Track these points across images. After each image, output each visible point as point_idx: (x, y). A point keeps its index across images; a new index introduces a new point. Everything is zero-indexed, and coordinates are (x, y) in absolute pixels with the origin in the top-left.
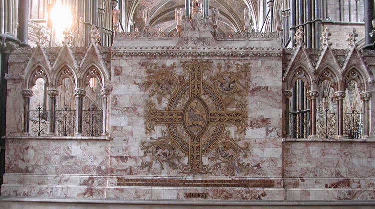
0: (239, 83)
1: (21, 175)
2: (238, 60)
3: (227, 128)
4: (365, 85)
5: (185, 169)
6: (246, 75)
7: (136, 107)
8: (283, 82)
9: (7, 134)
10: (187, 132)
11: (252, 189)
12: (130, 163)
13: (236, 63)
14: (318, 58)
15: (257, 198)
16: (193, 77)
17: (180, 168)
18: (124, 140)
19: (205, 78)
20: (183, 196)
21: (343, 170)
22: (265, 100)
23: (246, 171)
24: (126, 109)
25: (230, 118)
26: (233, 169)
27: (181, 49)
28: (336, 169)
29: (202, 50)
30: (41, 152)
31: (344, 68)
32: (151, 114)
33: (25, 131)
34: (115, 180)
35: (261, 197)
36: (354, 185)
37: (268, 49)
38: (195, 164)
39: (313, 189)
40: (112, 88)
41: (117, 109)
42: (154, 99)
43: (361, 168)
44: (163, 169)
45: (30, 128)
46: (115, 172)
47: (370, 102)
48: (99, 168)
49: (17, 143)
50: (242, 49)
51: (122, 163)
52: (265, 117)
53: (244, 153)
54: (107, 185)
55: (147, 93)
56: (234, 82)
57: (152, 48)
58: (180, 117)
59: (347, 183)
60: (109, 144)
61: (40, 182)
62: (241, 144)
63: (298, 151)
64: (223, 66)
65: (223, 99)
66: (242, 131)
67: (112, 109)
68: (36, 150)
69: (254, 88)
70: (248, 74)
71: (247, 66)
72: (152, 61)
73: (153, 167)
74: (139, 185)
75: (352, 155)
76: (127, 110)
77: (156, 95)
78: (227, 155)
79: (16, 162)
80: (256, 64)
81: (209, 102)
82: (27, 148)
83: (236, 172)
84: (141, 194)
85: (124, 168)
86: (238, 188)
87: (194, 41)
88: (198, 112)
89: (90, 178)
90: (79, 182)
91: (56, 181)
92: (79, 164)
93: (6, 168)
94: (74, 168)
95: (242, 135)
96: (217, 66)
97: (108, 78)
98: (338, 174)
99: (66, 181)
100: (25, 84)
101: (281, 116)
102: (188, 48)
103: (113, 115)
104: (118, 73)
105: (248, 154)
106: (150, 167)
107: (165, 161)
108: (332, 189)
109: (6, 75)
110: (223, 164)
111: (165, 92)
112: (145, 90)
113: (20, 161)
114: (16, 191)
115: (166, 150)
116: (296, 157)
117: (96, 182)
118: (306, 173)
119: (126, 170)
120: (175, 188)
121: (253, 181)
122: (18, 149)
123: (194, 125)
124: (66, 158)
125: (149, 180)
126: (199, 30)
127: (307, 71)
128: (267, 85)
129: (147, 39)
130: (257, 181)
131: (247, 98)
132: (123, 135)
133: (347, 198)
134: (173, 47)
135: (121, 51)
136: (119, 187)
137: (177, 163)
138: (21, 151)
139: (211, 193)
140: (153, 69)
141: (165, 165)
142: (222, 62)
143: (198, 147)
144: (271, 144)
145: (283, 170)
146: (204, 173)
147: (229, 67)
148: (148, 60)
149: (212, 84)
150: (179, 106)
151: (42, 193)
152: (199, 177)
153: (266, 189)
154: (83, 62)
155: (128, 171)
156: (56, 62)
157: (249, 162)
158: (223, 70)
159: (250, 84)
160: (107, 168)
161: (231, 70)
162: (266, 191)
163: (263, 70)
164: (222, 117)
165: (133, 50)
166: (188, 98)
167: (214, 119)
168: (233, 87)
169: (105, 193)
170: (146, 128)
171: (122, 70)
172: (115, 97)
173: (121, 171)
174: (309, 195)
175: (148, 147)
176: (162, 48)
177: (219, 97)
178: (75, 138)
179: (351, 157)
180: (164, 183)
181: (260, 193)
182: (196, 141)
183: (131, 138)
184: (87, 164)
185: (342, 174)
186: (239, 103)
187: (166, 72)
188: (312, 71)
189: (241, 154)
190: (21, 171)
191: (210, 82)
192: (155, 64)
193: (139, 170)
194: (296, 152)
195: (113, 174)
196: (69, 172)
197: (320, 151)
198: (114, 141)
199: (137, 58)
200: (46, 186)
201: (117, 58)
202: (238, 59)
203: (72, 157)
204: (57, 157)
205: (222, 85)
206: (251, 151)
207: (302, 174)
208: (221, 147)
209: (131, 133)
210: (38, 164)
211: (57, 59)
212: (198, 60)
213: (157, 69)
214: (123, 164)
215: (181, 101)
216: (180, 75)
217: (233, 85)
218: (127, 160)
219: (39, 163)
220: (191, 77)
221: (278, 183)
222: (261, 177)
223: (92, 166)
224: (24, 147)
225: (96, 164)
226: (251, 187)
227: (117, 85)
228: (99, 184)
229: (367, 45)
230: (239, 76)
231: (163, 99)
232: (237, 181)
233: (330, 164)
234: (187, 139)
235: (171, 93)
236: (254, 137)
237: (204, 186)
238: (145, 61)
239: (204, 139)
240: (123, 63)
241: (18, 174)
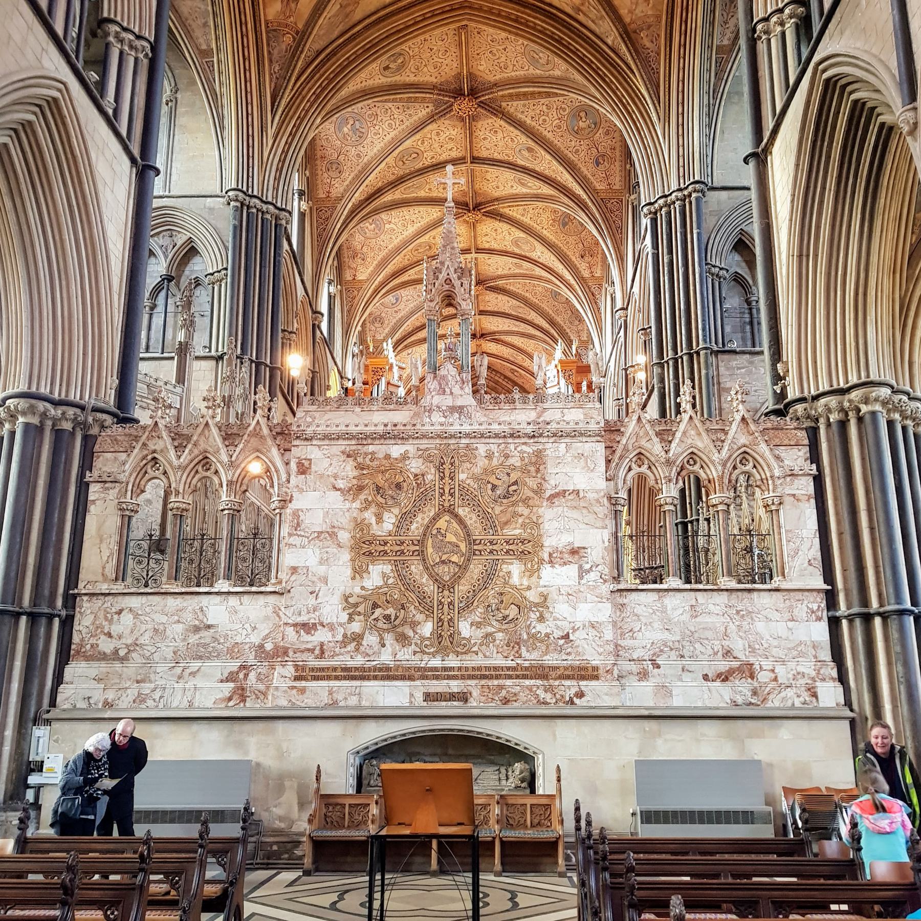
0: (525, 484)
1: (102, 667)
2: (523, 444)
3: (504, 566)
4: (770, 482)
5: (426, 646)
6: (538, 471)
7: (336, 530)
8: (607, 480)
9: (81, 585)
10: (431, 576)
11: (557, 683)
12: (321, 636)
13: (519, 449)
14: (674, 434)
15: (567, 703)
16: (442, 475)
17: (416, 644)
18: (311, 593)
19: (462, 476)
20: (422, 699)
21: (739, 646)
22: (575, 514)
23: (544, 648)
24: (316, 535)
25: (511, 547)
26: (518, 644)
27: (418, 427)
28: (724, 642)
29: (456, 428)
30: (147, 619)
31: (725, 453)
32: (364, 543)
33: (117, 579)
34: (290, 670)
35: (575, 699)
36: (764, 677)
37: (577, 423)
38: (445, 634)
39: (679, 684)
40: (292, 496)
41: (298, 536)
42: (369, 516)
43: (775, 643)
44: (383, 645)
45: (129, 572)
46: (291, 653)
47: (781, 512)
48: (261, 646)
49: (100, 603)
50: (529, 424)
51: (305, 637)
52: (576, 545)
53: (538, 614)
54: (275, 681)
55: (357, 504)
56: (513, 484)
57: (366, 426)
58: (417, 548)
59: (748, 671)
60: (281, 601)
61: (139, 678)
62: (532, 596)
63: (644, 609)
64: (496, 454)
65: (497, 513)
66: (533, 572)
67: (290, 535)
68: (136, 616)
69: (553, 492)
70: (541, 468)
71: (539, 454)
72: (366, 447)
73: (364, 643)
74: (337, 678)
75: (754, 615)
76: (318, 537)
77: (373, 509)
78: (505, 618)
80: (554, 450)
81: (471, 519)
82: (120, 612)
83: (523, 649)
84: (340, 697)
85: (310, 646)
86: (527, 682)
87: (443, 412)
88: (451, 538)
89: (243, 667)
90: (219, 677)
91: (173, 675)
92: (222, 641)
93: (72, 652)
95: (534, 579)
96: (484, 454)
97: (284, 480)
98: (728, 653)
99: (193, 674)
100: (124, 490)
101: (607, 544)
102: (432, 425)
103: (290, 545)
104: (303, 469)
105: (547, 615)
106: (359, 644)
107: (388, 631)
108: (718, 683)
109: (88, 474)
110: (500, 636)
111: (390, 502)
112: (354, 500)
113: (103, 637)
114: (89, 698)
115: (391, 610)
116: (639, 620)
117: (252, 676)
118: (661, 651)
119: (312, 651)
120: (408, 683)
121: (558, 668)
122: (101, 615)
123: (443, 562)
124: (197, 629)
125: (357, 669)
126: (452, 393)
127: (653, 459)
128: (577, 487)
129: (358, 409)
130: (566, 669)
131: (541, 511)
132: (310, 584)
133: (751, 704)
134: (405, 422)
135: (309, 431)
136: (297, 684)
137: (411, 634)
138: (106, 619)
139: (476, 693)
140: (369, 463)
141: (389, 638)
142: (494, 448)
143: (450, 603)
144: (589, 596)
145: (616, 645)
146: (462, 653)
147: (507, 457)
148: (360, 447)
149: (476, 486)
150: (416, 527)
151: (143, 701)
152: (453, 661)
153: (582, 683)
154: (238, 450)
155: (317, 652)
156: (187, 451)
157: (548, 631)
158: (495, 462)
159: (546, 486)
160: (276, 647)
161: (511, 461)
162: (583, 688)
163: (570, 459)
164: (495, 547)
165: (333, 429)
166: (432, 514)
167: (480, 551)
168: (515, 491)
169: (270, 697)
170: (355, 571)
171: (310, 464)
172: (296, 514)
173: (302, 652)
174: (671, 695)
175: (356, 605)
176: (386, 425)
177: (490, 511)
178: (216, 590)
179: (752, 619)
180: (386, 674)
181: (573, 691)
182: (446, 593)
183: (324, 588)
184: (239, 639)
185: (735, 654)
186: (527, 521)
187: (392, 465)
188: (663, 460)
189: (532, 615)
190: (103, 657)
191: (472, 484)
192: (373, 453)
193: (337, 650)
194: (639, 610)
195: (287, 659)
196: (200, 658)
197: (687, 608)
198: (291, 594)
199: (341, 442)
200: (152, 685)
201: (303, 443)
202: (523, 440)
203: (209, 627)
204: (179, 628)
205: (494, 488)
206: (551, 609)
207: (654, 654)
208: (494, 601)
209: (325, 580)
210: (138, 642)
211: (190, 446)
212: (449, 445)
213: (376, 463)
214: (308, 638)
215: (419, 519)
216: (417, 471)
217: (514, 488)
218: (316, 630)
219: (141, 641)
220: (437, 476)
221: (607, 671)
222: (573, 660)
223: (246, 643)
224: (114, 610)
225: (255, 639)
226: (555, 679)
227: (301, 491)
228: (259, 679)
229: (771, 408)
230: (524, 470)
231: (386, 516)
232: (526, 669)
233: (709, 634)
234: (430, 588)
235: (400, 505)
236: (558, 582)
237: (463, 677)
238: (354, 447)
239: (463, 588)
240: (312, 452)
241: (95, 664)
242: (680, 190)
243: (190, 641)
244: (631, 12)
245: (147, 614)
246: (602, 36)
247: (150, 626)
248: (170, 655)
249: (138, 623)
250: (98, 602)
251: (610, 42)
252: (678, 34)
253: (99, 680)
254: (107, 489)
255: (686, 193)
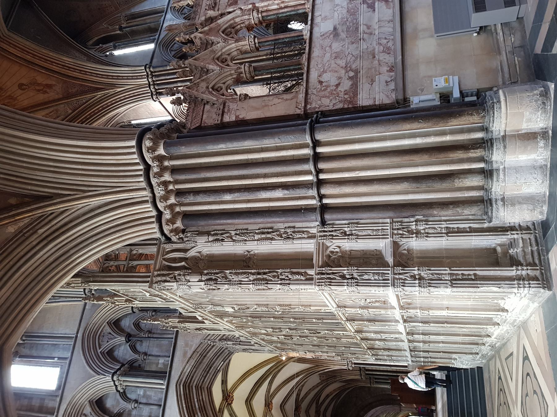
49: (313, 97)
68: (324, 72)
79: (342, 95)
82: (321, 82)
92: (346, 19)
94: (351, 24)
99: (369, 27)
113: (339, 89)
151: (389, 49)
184: (345, 11)
210: (344, 66)
219: (344, 65)
242: (148, 76)
243: (345, 36)
244: (58, 94)
245: (324, 65)
246: (66, 115)
247: (333, 62)
248: (355, 45)
249: (330, 69)
250: (312, 97)
251: (70, 111)
252: (74, 73)
253: (373, 81)
254: (229, 110)
255: (150, 73)
